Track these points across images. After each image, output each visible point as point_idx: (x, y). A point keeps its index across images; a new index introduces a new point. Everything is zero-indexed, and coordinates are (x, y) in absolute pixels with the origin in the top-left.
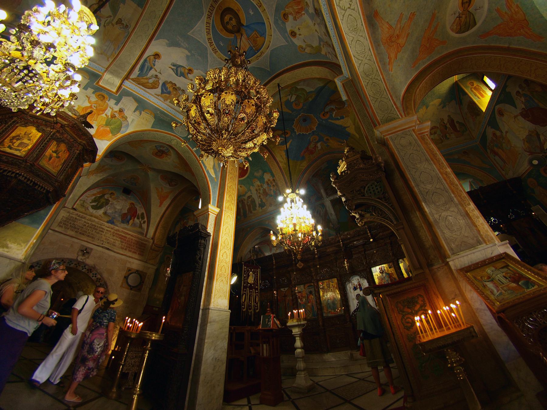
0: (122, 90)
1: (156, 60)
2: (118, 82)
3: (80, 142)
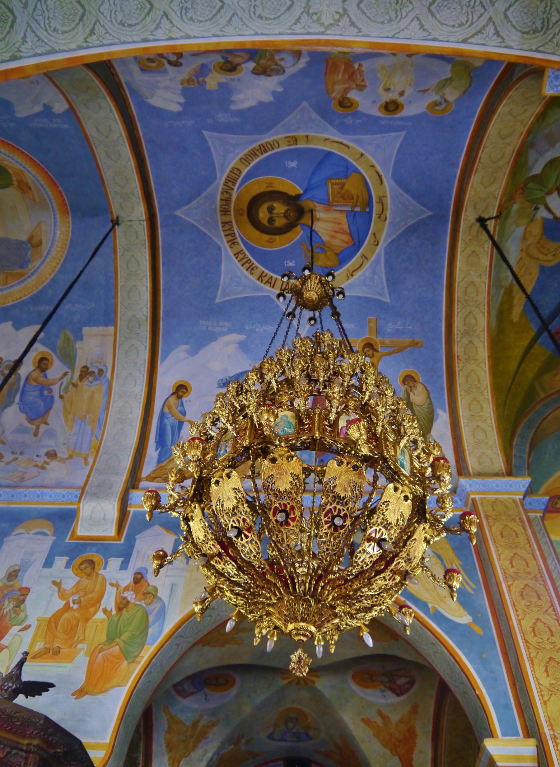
0: (131, 520)
1: (184, 399)
2: (114, 508)
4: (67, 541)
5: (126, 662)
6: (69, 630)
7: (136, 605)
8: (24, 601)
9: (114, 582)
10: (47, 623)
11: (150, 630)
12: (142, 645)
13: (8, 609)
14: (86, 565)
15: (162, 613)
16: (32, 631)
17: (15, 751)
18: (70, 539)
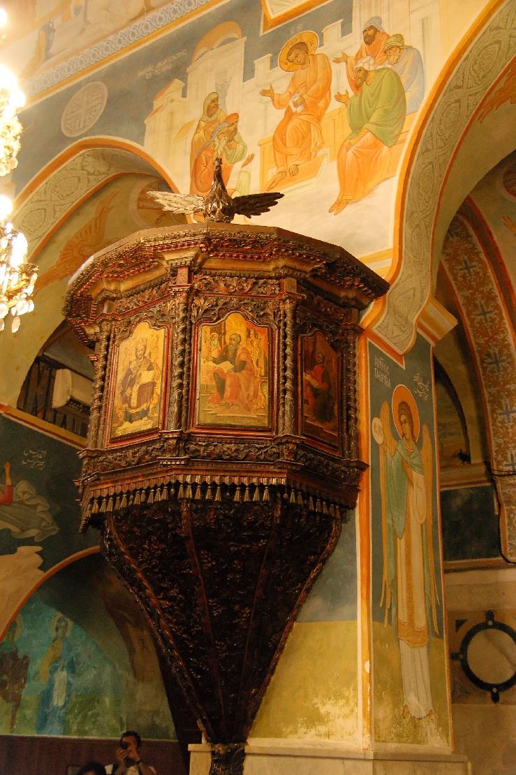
3: (274, 269)
4: (261, 34)
5: (386, 147)
6: (301, 137)
7: (378, 71)
8: (236, 129)
9: (339, 56)
10: (272, 143)
11: (408, 95)
12: (402, 117)
13: (221, 149)
14: (296, 52)
15: (418, 62)
16: (257, 160)
17: (261, 281)
18: (264, 31)
